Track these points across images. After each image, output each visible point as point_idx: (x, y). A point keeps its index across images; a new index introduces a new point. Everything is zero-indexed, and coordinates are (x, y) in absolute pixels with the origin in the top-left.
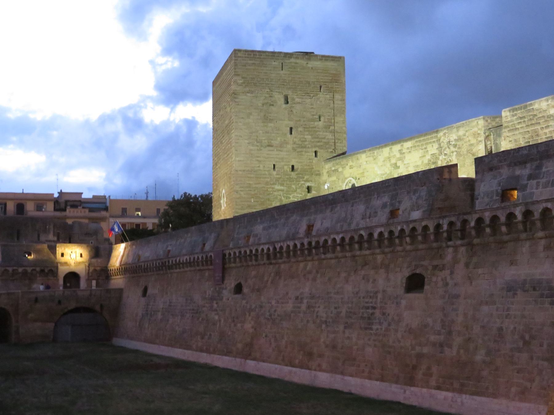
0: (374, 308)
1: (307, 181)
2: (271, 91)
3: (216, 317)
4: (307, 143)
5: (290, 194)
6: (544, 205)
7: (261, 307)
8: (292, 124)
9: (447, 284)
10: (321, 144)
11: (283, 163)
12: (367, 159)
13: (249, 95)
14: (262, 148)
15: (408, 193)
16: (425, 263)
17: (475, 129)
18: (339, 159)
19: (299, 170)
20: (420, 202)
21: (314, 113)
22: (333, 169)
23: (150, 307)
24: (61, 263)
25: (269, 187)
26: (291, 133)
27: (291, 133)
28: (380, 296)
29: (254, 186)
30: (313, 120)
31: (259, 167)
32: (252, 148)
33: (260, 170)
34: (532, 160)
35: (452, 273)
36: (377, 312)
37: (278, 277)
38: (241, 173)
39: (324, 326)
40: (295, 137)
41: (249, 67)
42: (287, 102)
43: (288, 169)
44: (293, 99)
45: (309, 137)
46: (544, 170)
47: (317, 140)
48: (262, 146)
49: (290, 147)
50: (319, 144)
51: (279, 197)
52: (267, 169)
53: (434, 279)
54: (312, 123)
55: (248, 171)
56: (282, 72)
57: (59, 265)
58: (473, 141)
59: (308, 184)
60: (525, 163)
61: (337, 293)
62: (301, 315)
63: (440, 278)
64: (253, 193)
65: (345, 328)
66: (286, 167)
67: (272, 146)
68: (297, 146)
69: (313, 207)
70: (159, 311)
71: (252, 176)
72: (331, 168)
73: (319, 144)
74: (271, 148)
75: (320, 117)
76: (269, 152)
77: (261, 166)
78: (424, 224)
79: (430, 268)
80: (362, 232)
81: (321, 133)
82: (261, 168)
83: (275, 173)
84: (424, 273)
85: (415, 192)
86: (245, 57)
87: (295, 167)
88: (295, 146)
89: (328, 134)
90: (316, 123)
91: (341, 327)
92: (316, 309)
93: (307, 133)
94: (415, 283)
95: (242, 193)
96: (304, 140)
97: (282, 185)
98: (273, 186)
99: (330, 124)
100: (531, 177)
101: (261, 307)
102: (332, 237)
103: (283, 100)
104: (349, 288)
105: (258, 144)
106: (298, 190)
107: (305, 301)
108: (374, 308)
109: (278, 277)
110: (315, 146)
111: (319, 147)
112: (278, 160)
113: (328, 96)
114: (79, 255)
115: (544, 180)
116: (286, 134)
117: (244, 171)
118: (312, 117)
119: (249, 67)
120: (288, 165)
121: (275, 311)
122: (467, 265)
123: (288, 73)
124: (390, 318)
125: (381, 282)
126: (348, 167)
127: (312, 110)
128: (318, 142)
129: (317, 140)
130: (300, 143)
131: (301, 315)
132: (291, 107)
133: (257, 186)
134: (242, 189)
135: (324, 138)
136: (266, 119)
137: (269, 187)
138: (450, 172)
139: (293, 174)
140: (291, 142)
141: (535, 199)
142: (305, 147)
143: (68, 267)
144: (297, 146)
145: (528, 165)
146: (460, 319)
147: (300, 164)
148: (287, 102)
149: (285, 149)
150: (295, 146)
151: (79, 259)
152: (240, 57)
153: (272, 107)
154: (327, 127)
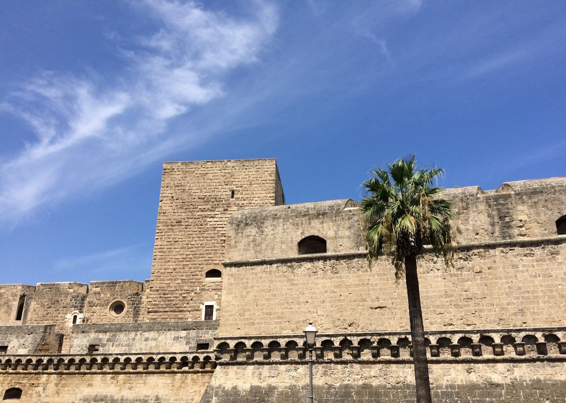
6: (116, 356)
9: (40, 396)
15: (17, 337)
16: (25, 381)
17: (15, 290)
20: (26, 344)
34: (111, 331)
35: (44, 389)
46: (117, 337)
53: (30, 392)
58: (11, 298)
60: (106, 332)
63: (34, 392)
78: (28, 358)
79: (28, 385)
84: (21, 388)
85: (23, 337)
100: (108, 340)
115: (117, 343)
122: (57, 385)
138: (51, 329)
141: (111, 352)
145: (108, 334)
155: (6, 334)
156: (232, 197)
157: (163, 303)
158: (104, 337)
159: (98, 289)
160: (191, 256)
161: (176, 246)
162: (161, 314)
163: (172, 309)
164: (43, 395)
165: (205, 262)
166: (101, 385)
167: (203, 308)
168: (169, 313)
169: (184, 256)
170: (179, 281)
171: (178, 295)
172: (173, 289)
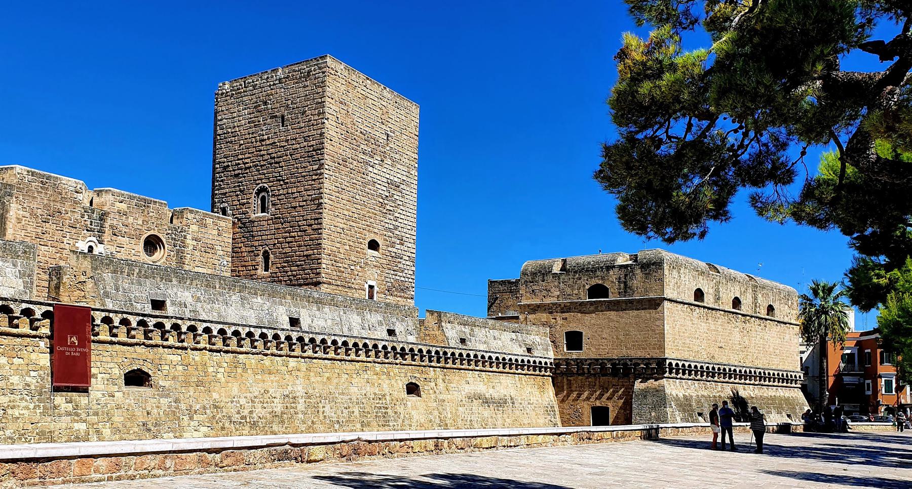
0: (387, 408)
3: (82, 427)
7: (204, 408)
28: (388, 398)
36: (389, 411)
37: (239, 370)
39: (337, 426)
61: (343, 394)
62: (300, 416)
65: (362, 426)
69: (289, 297)
80: (367, 341)
91: (359, 426)
92: (321, 410)
94: (413, 389)
101: (216, 407)
102: (333, 338)
104: (354, 390)
107: (301, 401)
108: (387, 408)
109: (239, 370)
121: (251, 412)
124: (402, 416)
125: (385, 386)
131: (300, 416)
146: (449, 416)
155: (385, 313)
156: (387, 144)
157: (335, 273)
158: (467, 330)
159: (123, 206)
160: (356, 216)
161: (344, 197)
162: (334, 287)
163: (343, 284)
164: (437, 392)
165: (368, 228)
166: (474, 382)
167: (367, 286)
168: (340, 288)
169: (351, 214)
170: (348, 247)
171: (346, 266)
172: (342, 256)
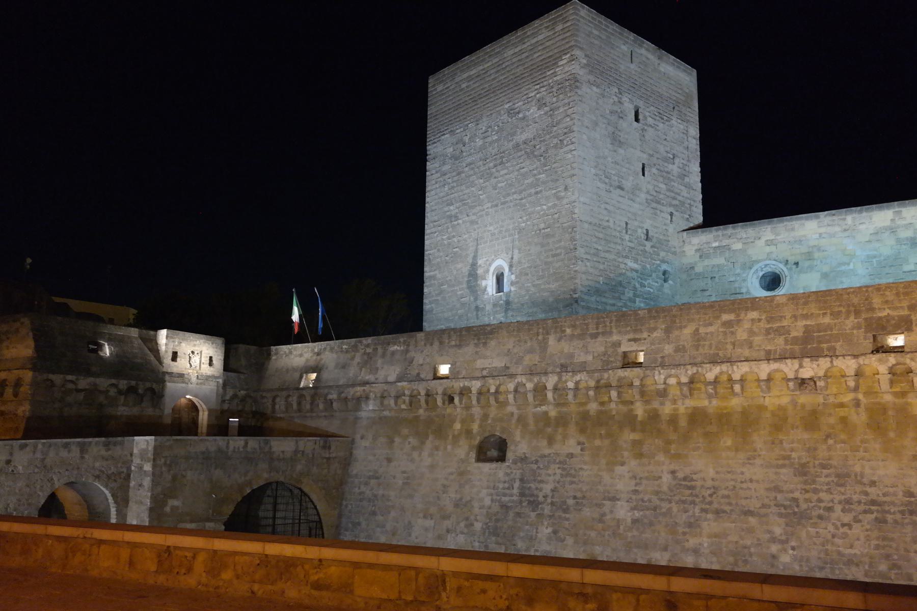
1: (663, 261)
2: (621, 94)
4: (661, 196)
5: (646, 280)
8: (644, 158)
10: (677, 202)
11: (636, 223)
12: (823, 230)
13: (594, 88)
14: (611, 189)
18: (717, 231)
19: (654, 240)
21: (668, 149)
22: (716, 244)
23: (547, 488)
24: (171, 374)
25: (620, 260)
26: (644, 175)
27: (644, 175)
29: (603, 255)
30: (666, 160)
31: (608, 221)
32: (599, 184)
33: (609, 227)
38: (586, 226)
40: (649, 182)
41: (593, 40)
42: (637, 120)
43: (641, 233)
44: (645, 118)
45: (663, 186)
47: (673, 195)
48: (611, 186)
49: (643, 196)
50: (675, 202)
51: (633, 282)
52: (618, 229)
54: (666, 164)
55: (595, 225)
56: (632, 66)
57: (167, 378)
59: (664, 267)
64: (601, 267)
66: (640, 230)
67: (622, 189)
68: (652, 198)
70: (614, 499)
71: (601, 235)
72: (708, 243)
73: (675, 202)
74: (622, 193)
75: (674, 155)
76: (621, 199)
77: (611, 221)
81: (676, 184)
82: (611, 224)
83: (627, 237)
86: (590, 21)
87: (650, 234)
88: (649, 197)
89: (683, 188)
90: (671, 166)
93: (661, 179)
95: (588, 264)
96: (658, 190)
97: (636, 261)
98: (626, 261)
99: (684, 172)
103: (632, 116)
105: (607, 180)
106: (654, 275)
110: (671, 205)
111: (675, 206)
112: (629, 215)
113: (682, 127)
114: (206, 360)
116: (638, 174)
117: (590, 223)
118: (665, 154)
119: (593, 40)
120: (642, 228)
123: (639, 70)
126: (761, 243)
127: (665, 142)
128: (674, 198)
129: (673, 195)
130: (655, 194)
132: (643, 130)
133: (607, 255)
134: (589, 257)
135: (679, 195)
136: (616, 141)
137: (620, 260)
139: (648, 244)
140: (644, 190)
142: (658, 203)
143: (184, 385)
144: (652, 198)
147: (655, 230)
148: (637, 120)
149: (638, 199)
150: (649, 197)
151: (206, 370)
152: (583, 18)
153: (621, 121)
154: (682, 176)
